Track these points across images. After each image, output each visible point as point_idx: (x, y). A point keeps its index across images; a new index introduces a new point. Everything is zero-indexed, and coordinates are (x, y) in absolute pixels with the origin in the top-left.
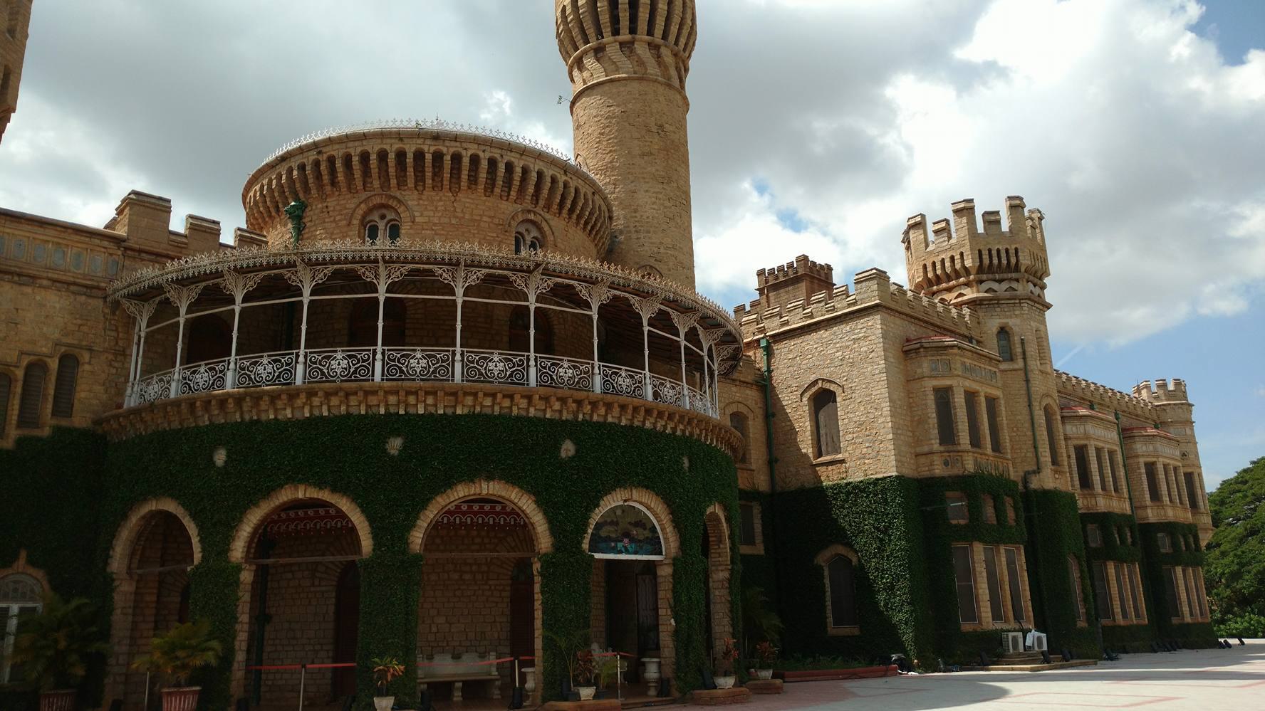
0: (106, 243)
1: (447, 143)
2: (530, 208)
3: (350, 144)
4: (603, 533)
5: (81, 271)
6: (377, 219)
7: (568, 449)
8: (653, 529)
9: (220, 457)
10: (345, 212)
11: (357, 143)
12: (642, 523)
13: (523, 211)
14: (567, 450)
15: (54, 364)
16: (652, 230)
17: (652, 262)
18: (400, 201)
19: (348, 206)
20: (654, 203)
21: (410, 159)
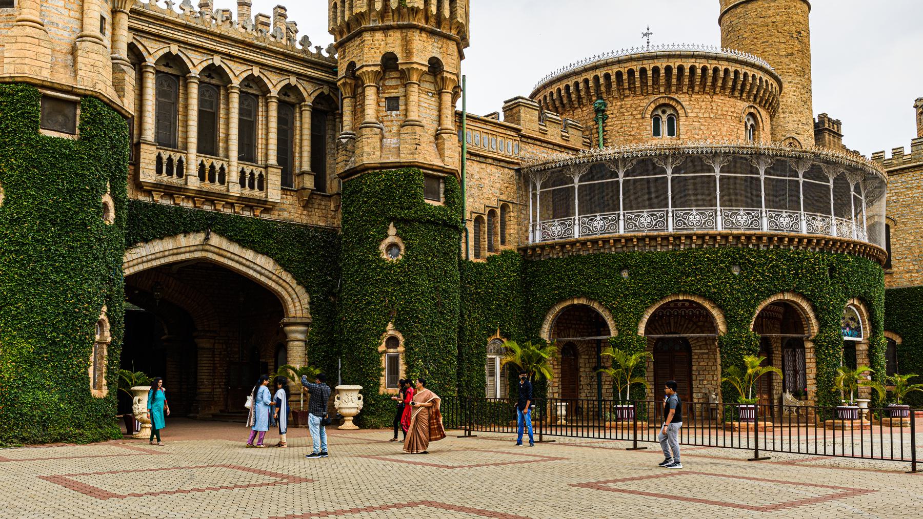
0: (512, 133)
1: (710, 62)
3: (645, 62)
5: (503, 152)
6: (661, 114)
10: (640, 108)
11: (650, 61)
15: (498, 211)
16: (793, 111)
17: (794, 135)
18: (677, 102)
19: (641, 105)
20: (795, 91)
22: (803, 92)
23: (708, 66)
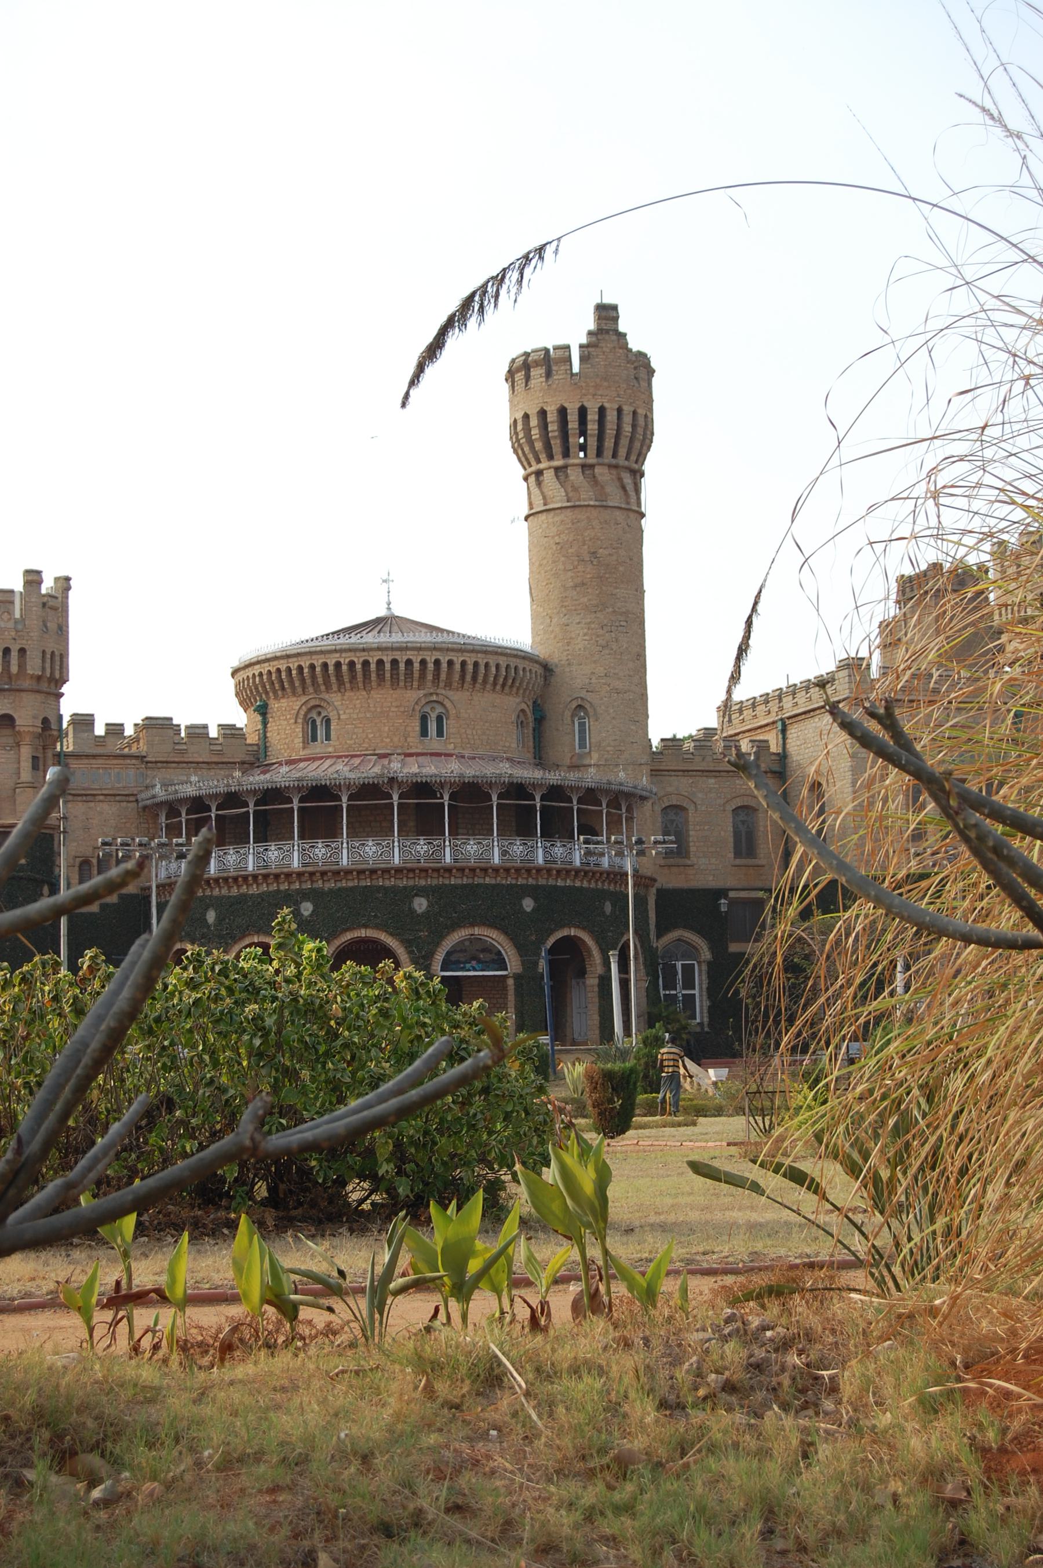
0: (134, 761)
1: (358, 654)
2: (432, 691)
4: (453, 958)
7: (420, 904)
8: (499, 953)
9: (211, 916)
12: (488, 949)
13: (425, 695)
14: (420, 905)
17: (583, 694)
20: (585, 635)
21: (331, 668)
22: (601, 632)
23: (356, 660)
